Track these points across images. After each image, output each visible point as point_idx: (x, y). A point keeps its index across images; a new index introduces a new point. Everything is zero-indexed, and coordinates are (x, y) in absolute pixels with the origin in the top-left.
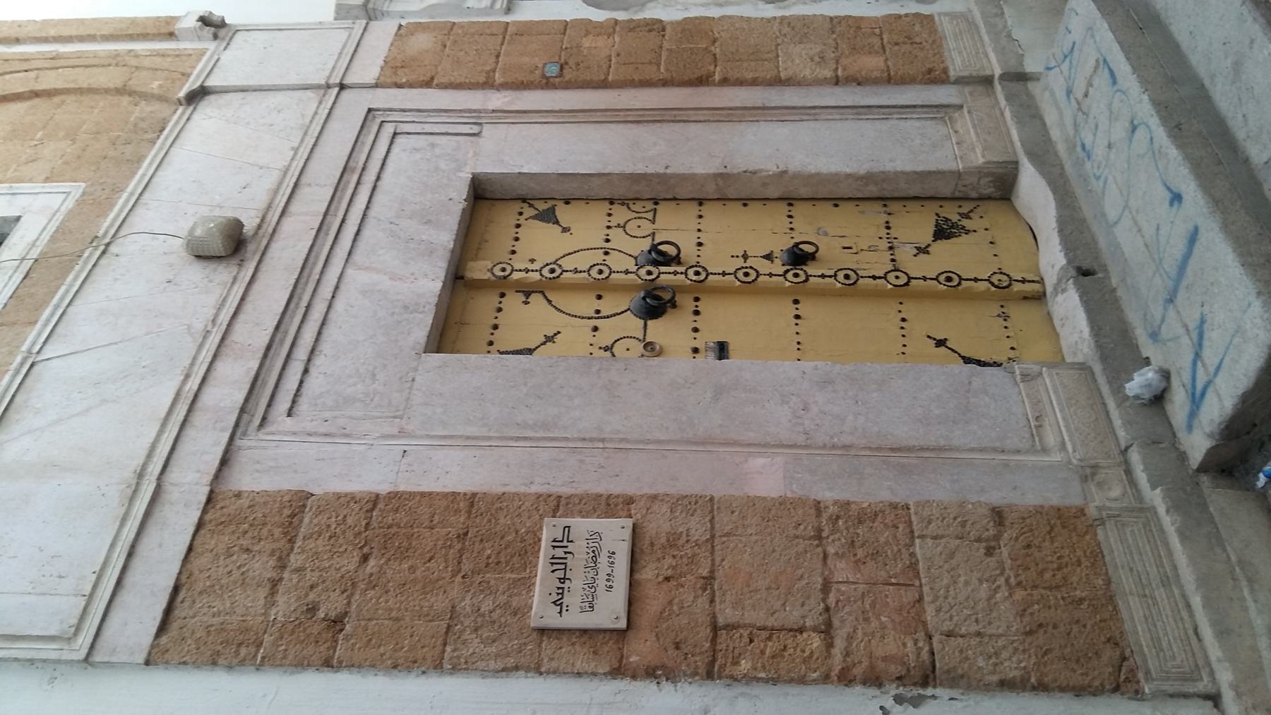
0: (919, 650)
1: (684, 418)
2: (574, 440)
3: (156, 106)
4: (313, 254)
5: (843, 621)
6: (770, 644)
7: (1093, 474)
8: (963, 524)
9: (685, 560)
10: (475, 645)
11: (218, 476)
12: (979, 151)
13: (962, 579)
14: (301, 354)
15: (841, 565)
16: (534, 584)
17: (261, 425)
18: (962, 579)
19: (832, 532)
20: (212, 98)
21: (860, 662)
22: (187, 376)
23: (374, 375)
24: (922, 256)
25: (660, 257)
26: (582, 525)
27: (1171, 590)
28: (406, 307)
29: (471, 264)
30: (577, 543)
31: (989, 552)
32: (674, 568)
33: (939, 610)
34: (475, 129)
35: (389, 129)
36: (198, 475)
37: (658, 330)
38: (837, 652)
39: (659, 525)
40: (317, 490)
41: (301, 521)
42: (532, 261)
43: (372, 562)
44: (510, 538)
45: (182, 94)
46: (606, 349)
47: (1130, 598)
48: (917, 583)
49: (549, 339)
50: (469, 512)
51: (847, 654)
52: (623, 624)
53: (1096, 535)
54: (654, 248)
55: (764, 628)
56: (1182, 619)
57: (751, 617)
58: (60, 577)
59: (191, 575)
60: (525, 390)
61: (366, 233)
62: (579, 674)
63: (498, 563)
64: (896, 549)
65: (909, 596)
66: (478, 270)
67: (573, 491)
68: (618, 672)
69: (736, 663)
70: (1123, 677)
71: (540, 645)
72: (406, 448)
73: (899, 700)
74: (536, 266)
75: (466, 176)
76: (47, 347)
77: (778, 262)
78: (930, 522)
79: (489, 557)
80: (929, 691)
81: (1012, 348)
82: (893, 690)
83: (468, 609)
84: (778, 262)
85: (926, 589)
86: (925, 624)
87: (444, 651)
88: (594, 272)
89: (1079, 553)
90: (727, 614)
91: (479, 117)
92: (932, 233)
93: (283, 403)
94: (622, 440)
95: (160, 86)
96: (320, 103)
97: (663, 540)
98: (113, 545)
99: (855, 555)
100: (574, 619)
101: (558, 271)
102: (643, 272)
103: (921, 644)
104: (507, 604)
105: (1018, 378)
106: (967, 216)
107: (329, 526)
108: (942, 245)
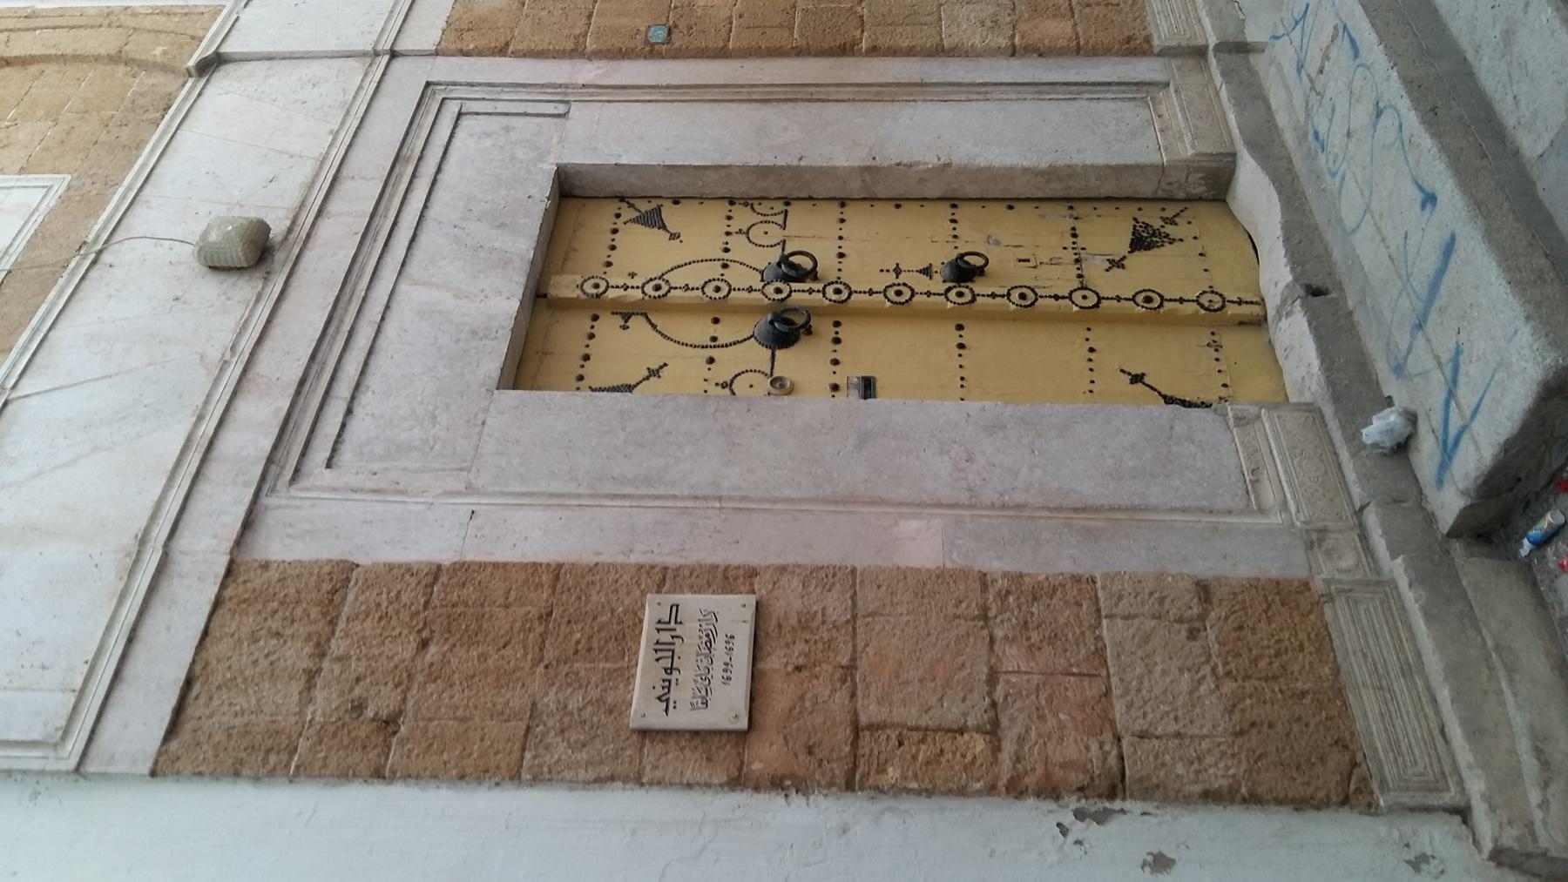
0: (1105, 755)
1: (820, 471)
2: (684, 498)
3: (159, 78)
4: (358, 265)
5: (1012, 720)
6: (923, 747)
7: (1320, 541)
8: (1161, 601)
9: (820, 645)
10: (560, 750)
11: (239, 542)
12: (1187, 140)
13: (1159, 668)
14: (343, 390)
15: (1012, 651)
16: (634, 676)
17: (294, 479)
18: (1159, 668)
19: (1001, 612)
20: (230, 67)
21: (1033, 769)
22: (200, 418)
23: (434, 417)
24: (1115, 270)
25: (792, 271)
26: (693, 603)
27: (1414, 683)
28: (474, 333)
29: (555, 279)
30: (687, 625)
31: (1193, 634)
32: (806, 655)
33: (1129, 706)
34: (561, 109)
35: (452, 109)
36: (215, 541)
37: (789, 362)
38: (1006, 756)
39: (788, 601)
40: (364, 560)
41: (344, 598)
42: (632, 275)
43: (433, 649)
44: (604, 618)
45: (192, 63)
47: (1363, 691)
48: (1104, 673)
49: (654, 373)
50: (554, 588)
51: (1018, 760)
52: (743, 724)
53: (1322, 614)
54: (784, 260)
55: (917, 728)
56: (1426, 716)
57: (900, 714)
58: (43, 668)
59: (207, 664)
60: (622, 436)
61: (424, 238)
62: (689, 786)
63: (589, 650)
64: (1078, 631)
65: (1093, 689)
66: (565, 286)
67: (683, 562)
68: (738, 781)
69: (881, 770)
70: (1352, 787)
71: (641, 750)
73: (1080, 815)
74: (638, 282)
75: (549, 168)
76: (23, 381)
77: (938, 278)
78: (1120, 598)
79: (578, 642)
80: (1117, 805)
81: (1225, 385)
82: (1073, 803)
83: (552, 707)
84: (938, 278)
85: (1114, 681)
86: (1112, 722)
87: (522, 758)
88: (709, 290)
89: (1302, 636)
90: (870, 711)
91: (566, 94)
93: (320, 452)
94: (743, 498)
95: (164, 53)
96: (366, 75)
97: (793, 621)
98: (109, 628)
99: (1029, 639)
100: (683, 718)
101: (665, 288)
102: (770, 289)
103: (1107, 747)
104: (601, 700)
105: (1231, 422)
106: (1171, 221)
107: (379, 604)
108: (1141, 257)
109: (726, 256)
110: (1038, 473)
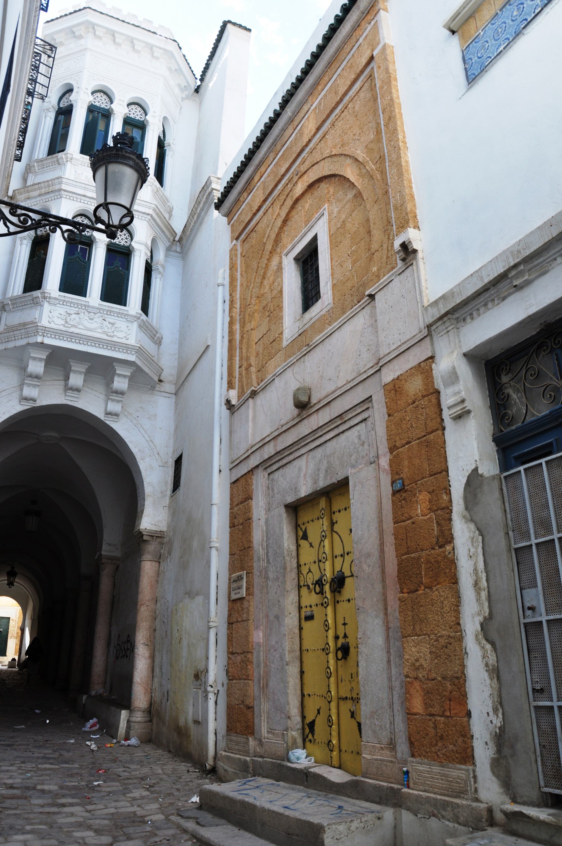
12: (368, 757)
24: (350, 714)
39: (245, 603)
77: (343, 641)
84: (343, 641)
93: (269, 470)
109: (346, 554)
110: (273, 670)
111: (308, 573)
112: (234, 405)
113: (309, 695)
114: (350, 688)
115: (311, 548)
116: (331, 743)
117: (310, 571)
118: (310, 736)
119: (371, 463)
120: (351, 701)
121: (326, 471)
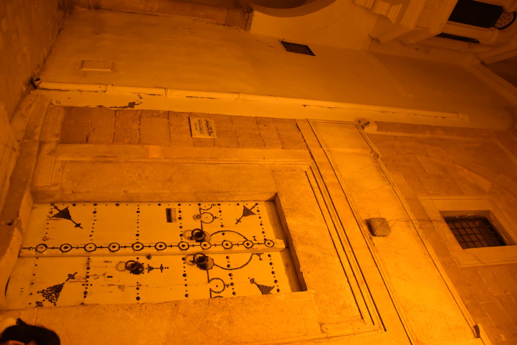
14: (317, 190)
26: (205, 136)
28: (294, 210)
37: (197, 225)
46: (215, 218)
49: (238, 221)
72: (265, 160)
77: (145, 266)
92: (62, 290)
101: (245, 244)
111: (212, 215)
112: (363, 128)
113: (95, 212)
114: (98, 274)
115: (235, 221)
116: (44, 248)
117: (215, 218)
118: (56, 212)
119: (321, 325)
120: (85, 276)
121: (310, 256)
